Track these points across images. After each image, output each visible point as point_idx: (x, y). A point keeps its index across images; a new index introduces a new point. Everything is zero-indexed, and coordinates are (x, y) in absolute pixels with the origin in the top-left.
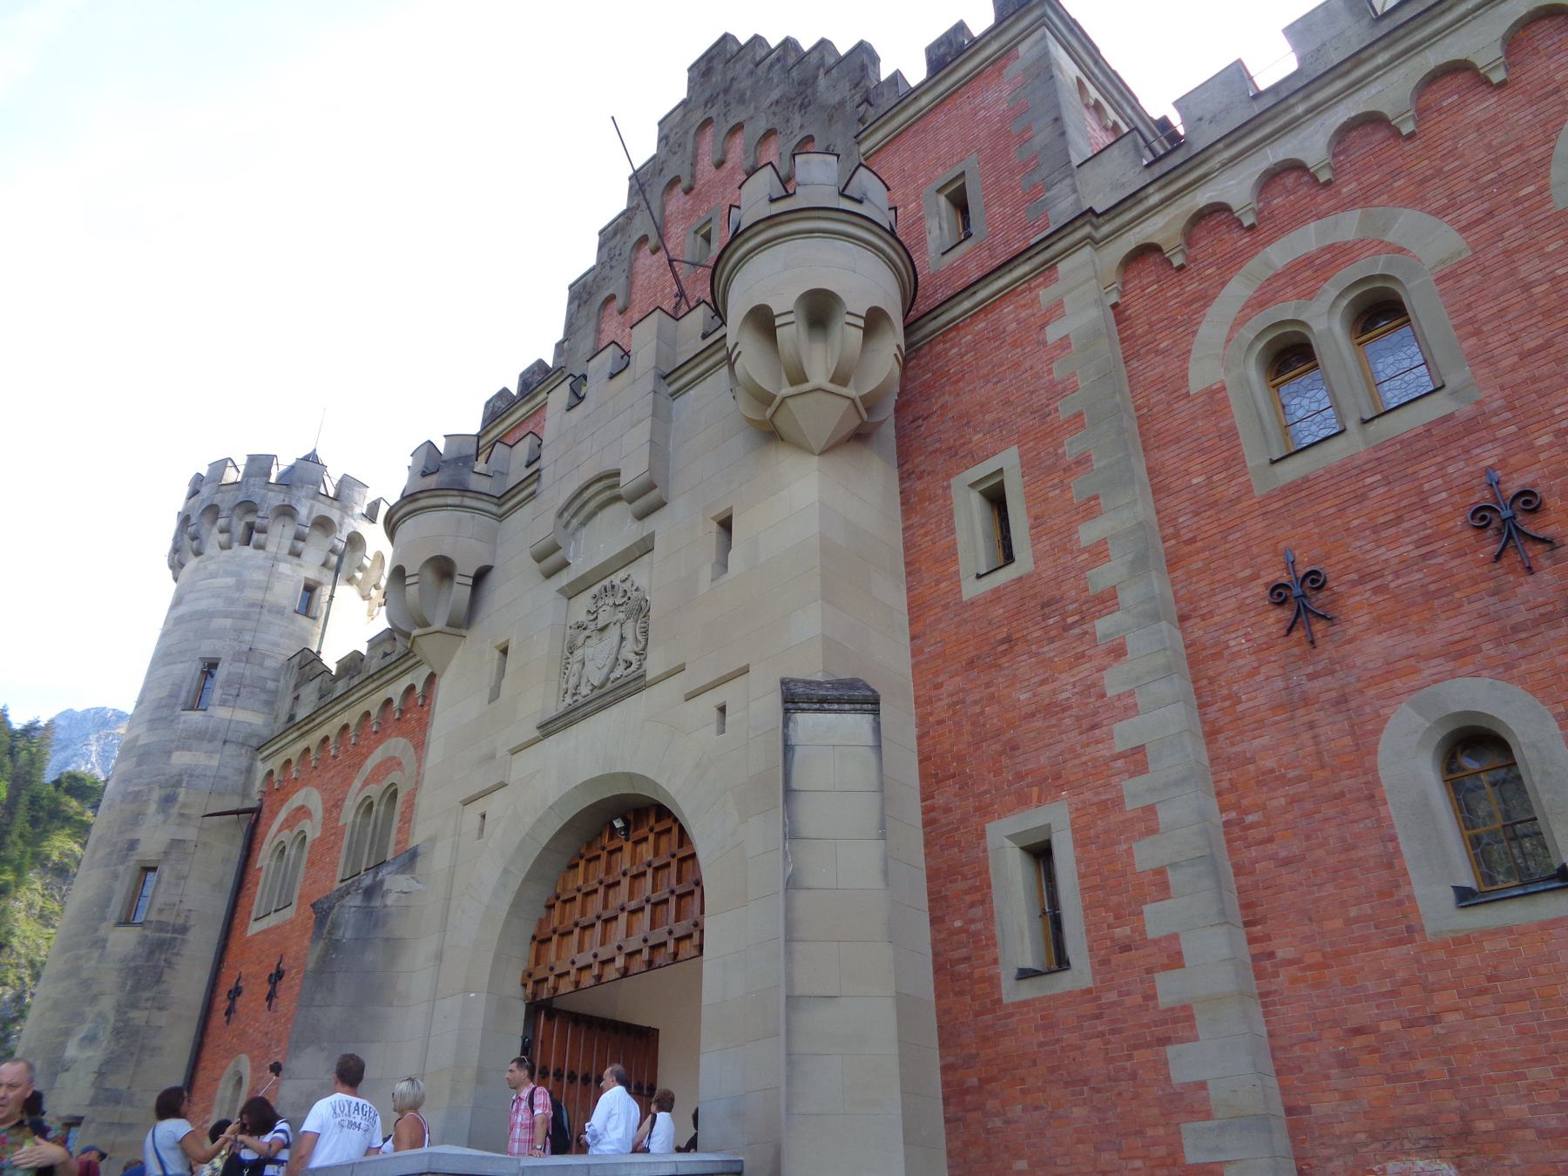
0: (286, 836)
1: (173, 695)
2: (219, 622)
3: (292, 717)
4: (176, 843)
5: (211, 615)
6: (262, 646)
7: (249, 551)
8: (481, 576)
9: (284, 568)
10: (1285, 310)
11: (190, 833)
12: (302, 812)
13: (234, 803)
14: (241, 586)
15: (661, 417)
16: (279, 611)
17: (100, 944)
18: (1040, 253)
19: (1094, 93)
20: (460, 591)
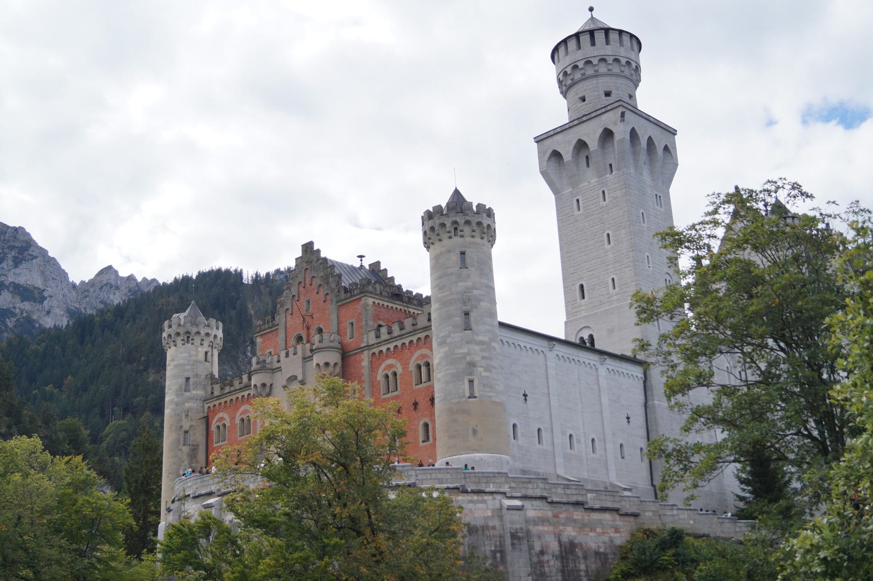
0: (218, 424)
1: (180, 388)
2: (187, 367)
3: (212, 393)
4: (191, 426)
5: (183, 365)
6: (199, 373)
7: (190, 345)
8: (271, 385)
9: (200, 349)
10: (386, 372)
11: (194, 423)
12: (222, 419)
13: (202, 415)
14: (190, 356)
15: (304, 367)
16: (201, 362)
17: (180, 450)
18: (362, 350)
19: (377, 301)
20: (268, 389)
